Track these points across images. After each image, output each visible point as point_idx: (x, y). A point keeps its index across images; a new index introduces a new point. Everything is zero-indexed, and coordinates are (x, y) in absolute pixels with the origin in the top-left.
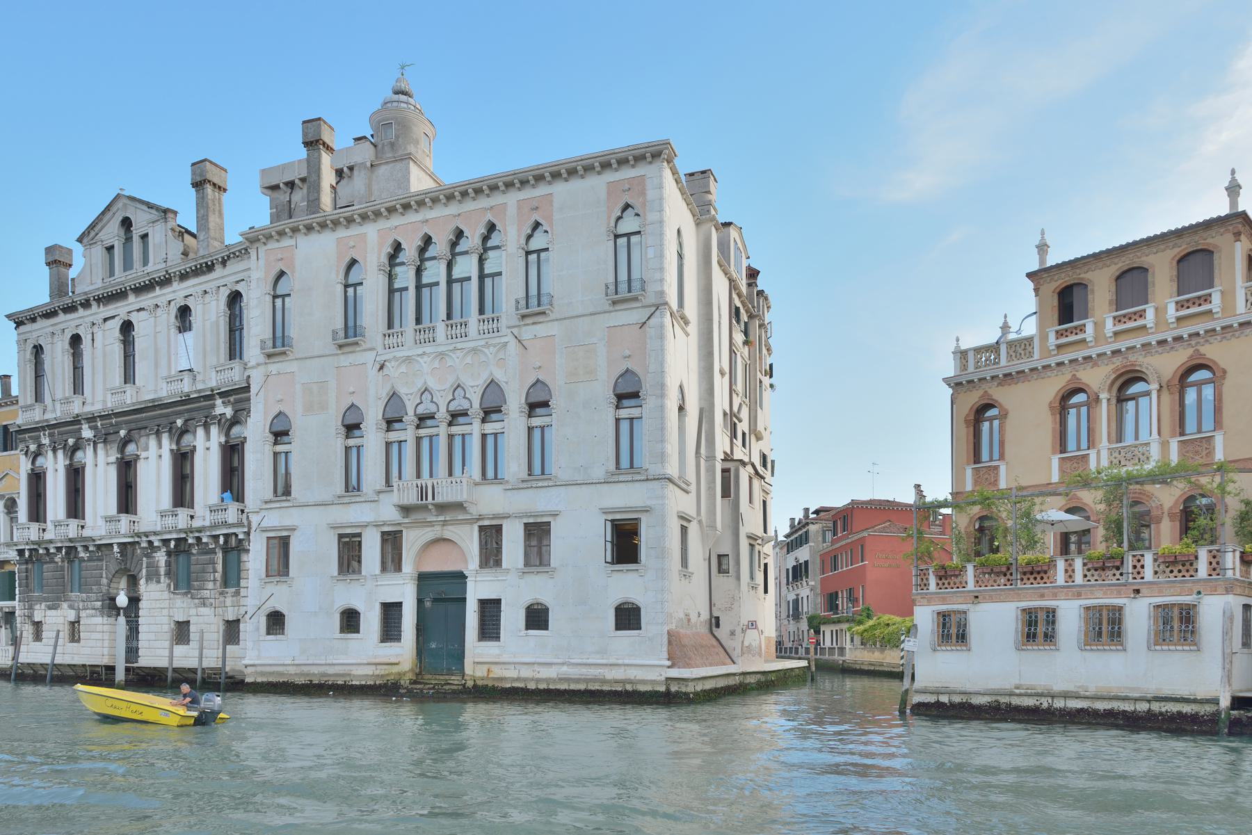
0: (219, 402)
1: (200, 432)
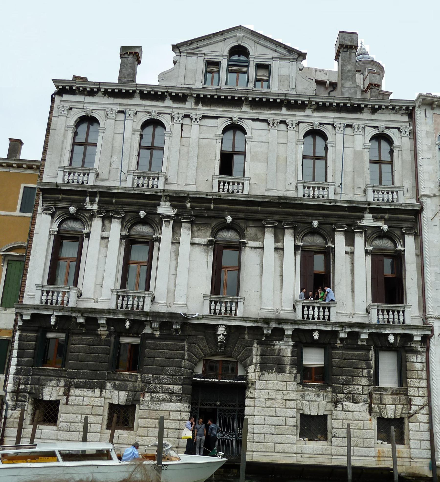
0: (368, 216)
1: (340, 239)
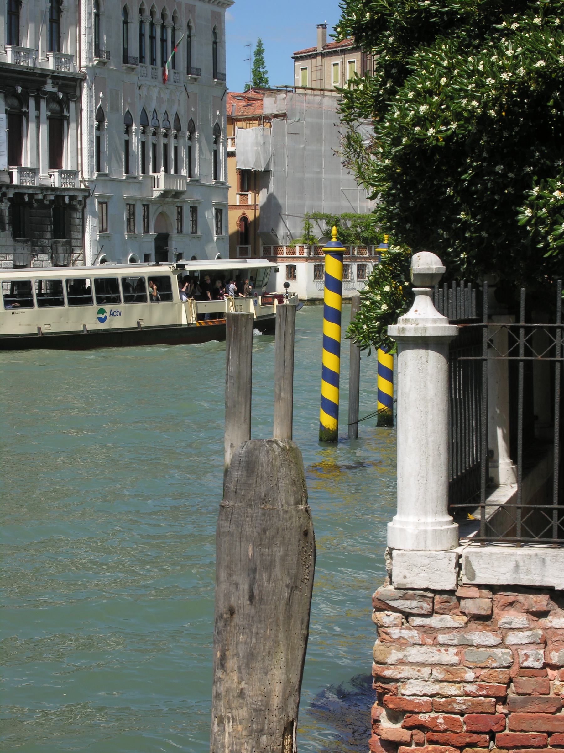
1: (32, 103)
